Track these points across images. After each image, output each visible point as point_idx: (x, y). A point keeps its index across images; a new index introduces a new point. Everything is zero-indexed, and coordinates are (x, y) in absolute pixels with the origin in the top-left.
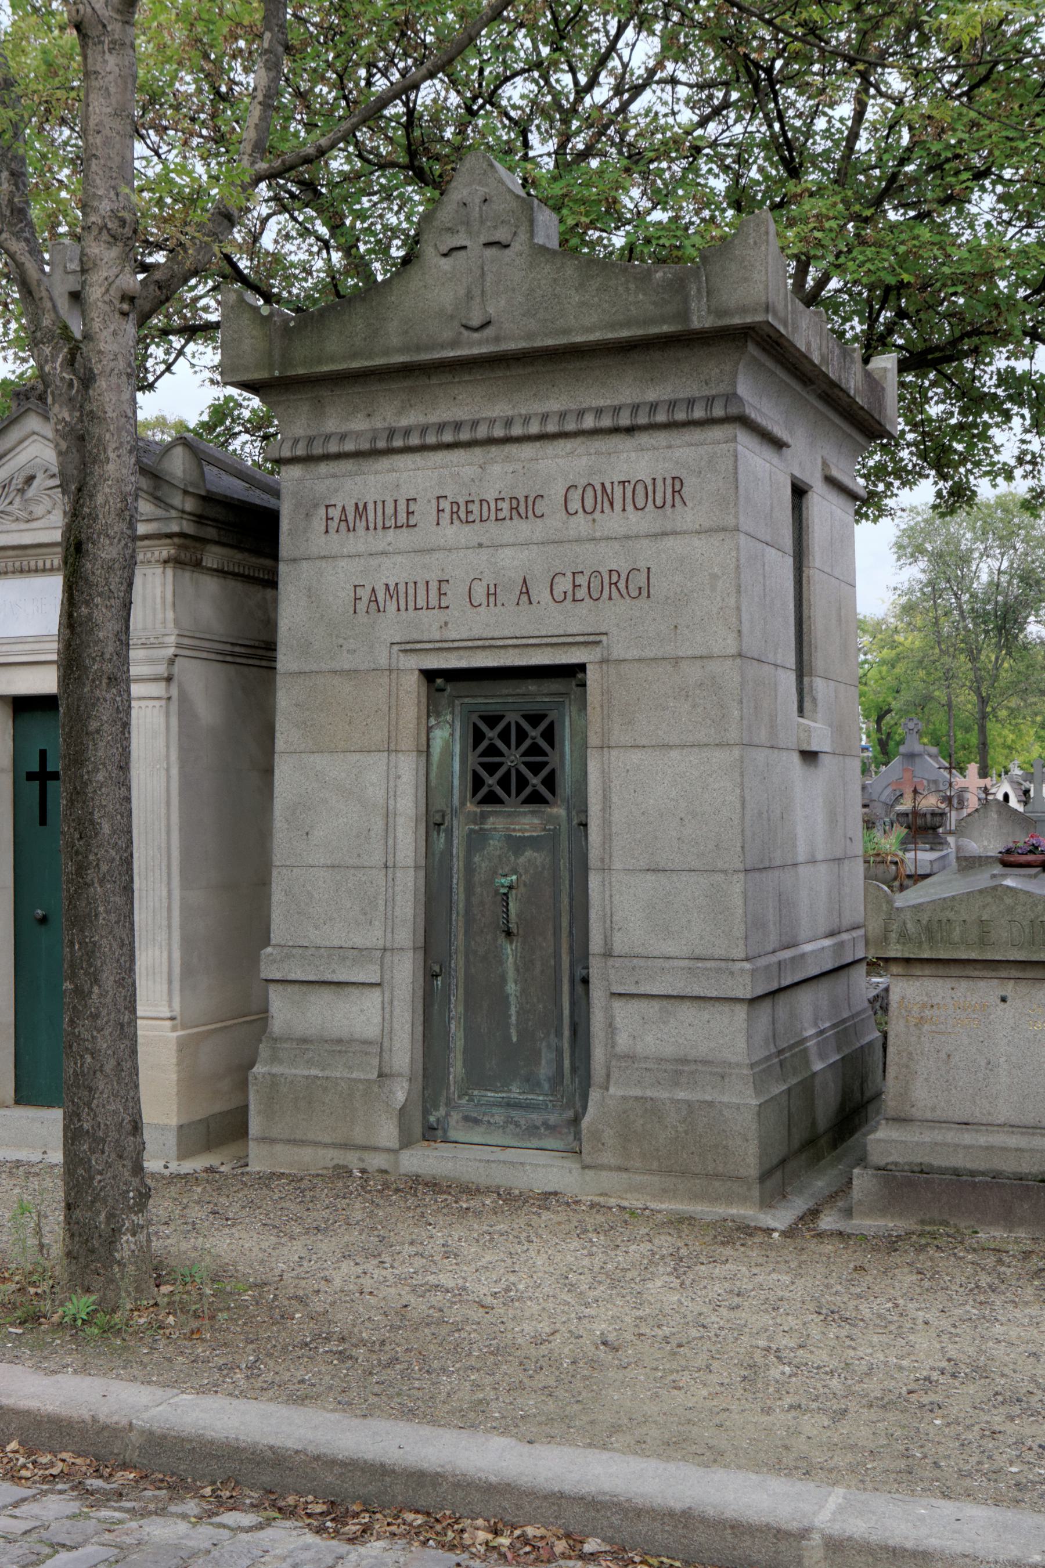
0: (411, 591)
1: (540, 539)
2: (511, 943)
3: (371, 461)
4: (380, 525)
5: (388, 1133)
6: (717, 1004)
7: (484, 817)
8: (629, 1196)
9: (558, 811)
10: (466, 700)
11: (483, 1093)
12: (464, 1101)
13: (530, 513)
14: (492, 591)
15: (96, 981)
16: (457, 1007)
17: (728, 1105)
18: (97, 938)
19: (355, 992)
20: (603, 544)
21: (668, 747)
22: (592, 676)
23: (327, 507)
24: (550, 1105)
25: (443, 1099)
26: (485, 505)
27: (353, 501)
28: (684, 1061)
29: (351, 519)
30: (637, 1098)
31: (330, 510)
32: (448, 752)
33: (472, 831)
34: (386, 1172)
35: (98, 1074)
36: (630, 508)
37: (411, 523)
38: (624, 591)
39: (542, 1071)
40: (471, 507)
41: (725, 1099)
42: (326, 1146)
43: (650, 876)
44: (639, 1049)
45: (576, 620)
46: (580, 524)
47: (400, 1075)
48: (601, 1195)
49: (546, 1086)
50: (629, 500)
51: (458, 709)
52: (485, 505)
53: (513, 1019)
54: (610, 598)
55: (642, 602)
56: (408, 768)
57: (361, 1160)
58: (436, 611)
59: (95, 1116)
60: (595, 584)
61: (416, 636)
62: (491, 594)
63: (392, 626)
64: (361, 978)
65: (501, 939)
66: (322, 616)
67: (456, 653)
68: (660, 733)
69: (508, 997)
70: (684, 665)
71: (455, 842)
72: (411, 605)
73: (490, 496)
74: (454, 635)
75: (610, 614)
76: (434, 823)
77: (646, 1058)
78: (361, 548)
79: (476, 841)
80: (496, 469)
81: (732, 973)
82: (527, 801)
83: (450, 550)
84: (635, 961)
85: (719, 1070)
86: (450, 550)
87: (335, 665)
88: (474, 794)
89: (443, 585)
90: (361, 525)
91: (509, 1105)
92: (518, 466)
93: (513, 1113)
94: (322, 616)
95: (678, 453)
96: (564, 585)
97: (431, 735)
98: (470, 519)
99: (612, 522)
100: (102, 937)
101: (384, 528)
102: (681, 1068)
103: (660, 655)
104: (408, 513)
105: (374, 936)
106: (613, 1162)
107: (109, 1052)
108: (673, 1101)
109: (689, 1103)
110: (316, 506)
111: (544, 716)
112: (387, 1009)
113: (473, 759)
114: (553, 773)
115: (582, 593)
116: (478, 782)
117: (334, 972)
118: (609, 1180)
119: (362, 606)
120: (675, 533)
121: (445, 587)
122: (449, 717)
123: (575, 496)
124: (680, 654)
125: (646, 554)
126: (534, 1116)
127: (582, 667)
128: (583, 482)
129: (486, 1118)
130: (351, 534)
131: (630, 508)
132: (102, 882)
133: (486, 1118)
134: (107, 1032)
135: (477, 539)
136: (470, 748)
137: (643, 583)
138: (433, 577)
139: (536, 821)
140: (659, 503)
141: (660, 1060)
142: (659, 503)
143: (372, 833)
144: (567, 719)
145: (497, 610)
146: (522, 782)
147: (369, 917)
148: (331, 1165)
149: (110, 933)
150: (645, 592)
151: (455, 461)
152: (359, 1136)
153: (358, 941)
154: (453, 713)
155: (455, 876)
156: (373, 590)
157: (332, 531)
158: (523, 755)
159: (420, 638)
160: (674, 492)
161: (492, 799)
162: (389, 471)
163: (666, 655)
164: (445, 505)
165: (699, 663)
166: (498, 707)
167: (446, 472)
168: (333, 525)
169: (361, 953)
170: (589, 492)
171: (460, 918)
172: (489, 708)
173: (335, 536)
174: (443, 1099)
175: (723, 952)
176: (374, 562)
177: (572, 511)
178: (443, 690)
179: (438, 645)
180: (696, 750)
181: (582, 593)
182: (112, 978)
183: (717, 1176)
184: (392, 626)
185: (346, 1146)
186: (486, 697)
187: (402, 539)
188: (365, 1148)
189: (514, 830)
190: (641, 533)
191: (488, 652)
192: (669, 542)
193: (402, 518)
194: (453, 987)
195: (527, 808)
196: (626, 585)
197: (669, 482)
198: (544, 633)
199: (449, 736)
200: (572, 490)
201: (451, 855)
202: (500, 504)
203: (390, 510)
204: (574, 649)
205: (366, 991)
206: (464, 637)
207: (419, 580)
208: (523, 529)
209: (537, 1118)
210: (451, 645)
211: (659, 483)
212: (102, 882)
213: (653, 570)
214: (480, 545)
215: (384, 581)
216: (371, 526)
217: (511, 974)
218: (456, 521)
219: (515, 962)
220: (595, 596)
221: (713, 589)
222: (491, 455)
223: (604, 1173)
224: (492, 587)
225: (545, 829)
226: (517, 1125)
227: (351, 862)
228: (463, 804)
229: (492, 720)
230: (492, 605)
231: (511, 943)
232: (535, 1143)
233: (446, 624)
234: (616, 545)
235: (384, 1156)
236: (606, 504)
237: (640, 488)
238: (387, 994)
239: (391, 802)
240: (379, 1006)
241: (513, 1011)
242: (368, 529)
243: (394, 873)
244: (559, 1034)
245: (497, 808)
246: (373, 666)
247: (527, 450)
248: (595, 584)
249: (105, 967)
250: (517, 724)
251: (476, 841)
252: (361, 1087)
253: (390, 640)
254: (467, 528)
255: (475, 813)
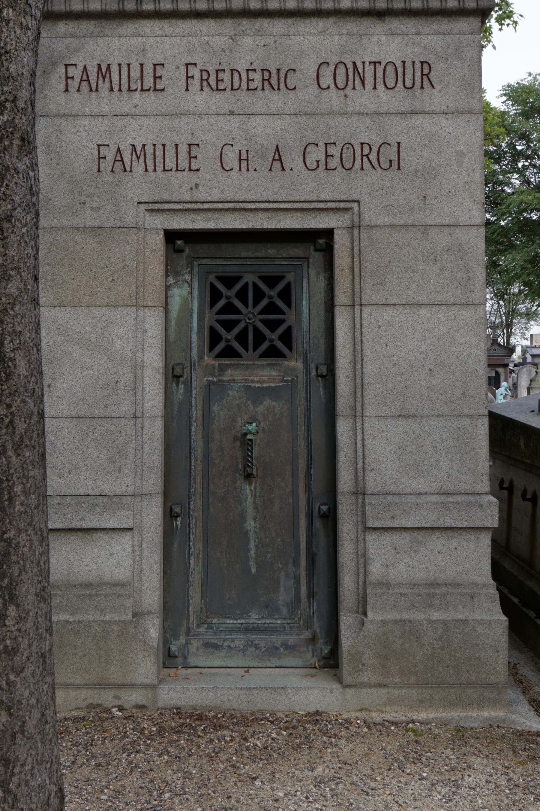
0: (159, 153)
1: (292, 111)
2: (250, 484)
3: (114, 24)
4: (125, 87)
5: (145, 669)
6: (464, 533)
7: (222, 369)
8: (388, 708)
9: (296, 364)
10: (204, 262)
11: (222, 620)
12: (202, 629)
13: (282, 85)
14: (244, 156)
15: (13, 598)
16: (196, 545)
17: (480, 622)
18: (11, 534)
19: (104, 537)
20: (354, 118)
21: (420, 305)
22: (341, 241)
23: (66, 66)
24: (287, 627)
25: (183, 629)
26: (236, 75)
27: (96, 62)
28: (435, 585)
29: (93, 79)
30: (396, 622)
31: (70, 69)
32: (186, 309)
33: (210, 383)
34: (143, 707)
35: (19, 736)
36: (380, 86)
37: (158, 87)
38: (375, 163)
39: (281, 598)
40: (221, 75)
41: (477, 616)
42: (78, 687)
43: (400, 421)
44: (392, 575)
45: (331, 186)
46: (332, 99)
47: (150, 613)
48: (361, 710)
49: (284, 611)
50: (380, 80)
51: (196, 270)
52: (236, 75)
53: (253, 552)
54: (362, 169)
55: (393, 173)
56: (153, 321)
57: (116, 697)
58: (186, 173)
59: (16, 800)
60: (347, 155)
61: (165, 196)
62: (243, 160)
63: (139, 185)
64: (112, 524)
65: (240, 481)
66: (63, 173)
67: (203, 215)
68: (410, 293)
69: (247, 533)
70: (433, 232)
71: (194, 393)
72: (159, 166)
73: (242, 66)
74: (204, 197)
75: (363, 185)
76: (173, 375)
77: (400, 584)
78: (105, 108)
79: (213, 391)
80: (248, 41)
81: (481, 506)
82: (265, 355)
83: (200, 116)
84: (389, 497)
85: (468, 591)
86: (200, 116)
87: (78, 222)
88: (211, 348)
89: (193, 148)
90: (104, 87)
91: (247, 630)
92: (270, 40)
93: (252, 637)
94: (63, 173)
95: (426, 40)
96: (316, 154)
97: (170, 293)
98: (221, 87)
99: (363, 99)
100: (19, 531)
101: (129, 90)
102: (434, 591)
103: (410, 222)
104: (155, 78)
105: (124, 483)
106: (373, 679)
107: (33, 701)
108: (430, 622)
109: (444, 622)
110: (54, 64)
111: (281, 278)
112: (137, 550)
113: (210, 317)
114: (289, 329)
115: (334, 163)
116: (215, 338)
117: (82, 519)
118: (369, 696)
119: (107, 165)
120: (423, 112)
121: (195, 151)
122: (188, 277)
123: (327, 72)
124: (429, 222)
125: (396, 130)
126: (274, 638)
127: (329, 233)
128: (335, 59)
129: (226, 644)
130: (94, 94)
131: (380, 86)
132: (18, 448)
133: (226, 644)
134: (27, 673)
135: (227, 107)
136: (207, 306)
137: (394, 157)
138: (183, 141)
139: (274, 373)
140: (408, 84)
141: (413, 585)
142: (408, 84)
143: (120, 385)
144: (305, 281)
145: (249, 175)
146: (259, 338)
147: (117, 465)
148: (84, 704)
149: (30, 524)
150: (396, 164)
151: (205, 32)
152: (114, 674)
153: (106, 488)
154: (191, 273)
155: (194, 424)
156: (119, 150)
157: (72, 90)
158: (260, 313)
159: (169, 198)
160: (422, 75)
161: (229, 353)
162: (134, 35)
163: (416, 223)
164: (195, 72)
165: (446, 231)
166: (235, 269)
167: (195, 40)
168: (74, 84)
169: (113, 501)
170: (341, 70)
171: (199, 462)
172: (228, 269)
173: (76, 96)
174: (183, 629)
175: (469, 487)
176: (119, 123)
177: (324, 86)
178: (182, 251)
179: (187, 206)
180: (444, 308)
181: (334, 163)
182: (32, 591)
183: (470, 684)
184: (139, 185)
185: (101, 685)
186: (224, 259)
187: (150, 102)
188: (121, 686)
189: (253, 381)
190: (392, 111)
191: (236, 215)
192: (418, 120)
193: (149, 82)
194: (192, 526)
195: (264, 362)
196: (380, 157)
197: (418, 65)
198: (296, 198)
199: (186, 294)
200: (324, 66)
201: (191, 405)
202: (252, 75)
203: (135, 73)
204: (322, 215)
205: (116, 536)
206: (215, 199)
207: (167, 142)
208: (275, 100)
209: (276, 640)
210: (200, 206)
211: (409, 66)
212: (18, 448)
213: (403, 145)
214: (231, 113)
215: (131, 141)
216: (116, 87)
217: (250, 512)
218: (206, 88)
219: (254, 502)
220: (347, 166)
221: (460, 164)
222: (241, 28)
223: (364, 691)
224: (244, 153)
225: (283, 381)
226: (257, 647)
227: (97, 413)
228: (201, 357)
229: (229, 281)
230: (244, 169)
231: (250, 484)
232: (275, 662)
233: (197, 186)
234: (368, 121)
235: (142, 692)
236: (358, 82)
237: (390, 70)
238: (136, 538)
239: (139, 355)
240: (130, 550)
241: (252, 545)
242: (112, 90)
243: (142, 423)
244: (296, 564)
245: (235, 361)
246: (118, 224)
247: (279, 26)
248: (347, 155)
249: (24, 577)
250: (254, 284)
251: (213, 391)
252: (116, 628)
253: (136, 199)
254: (218, 96)
255: (213, 366)
